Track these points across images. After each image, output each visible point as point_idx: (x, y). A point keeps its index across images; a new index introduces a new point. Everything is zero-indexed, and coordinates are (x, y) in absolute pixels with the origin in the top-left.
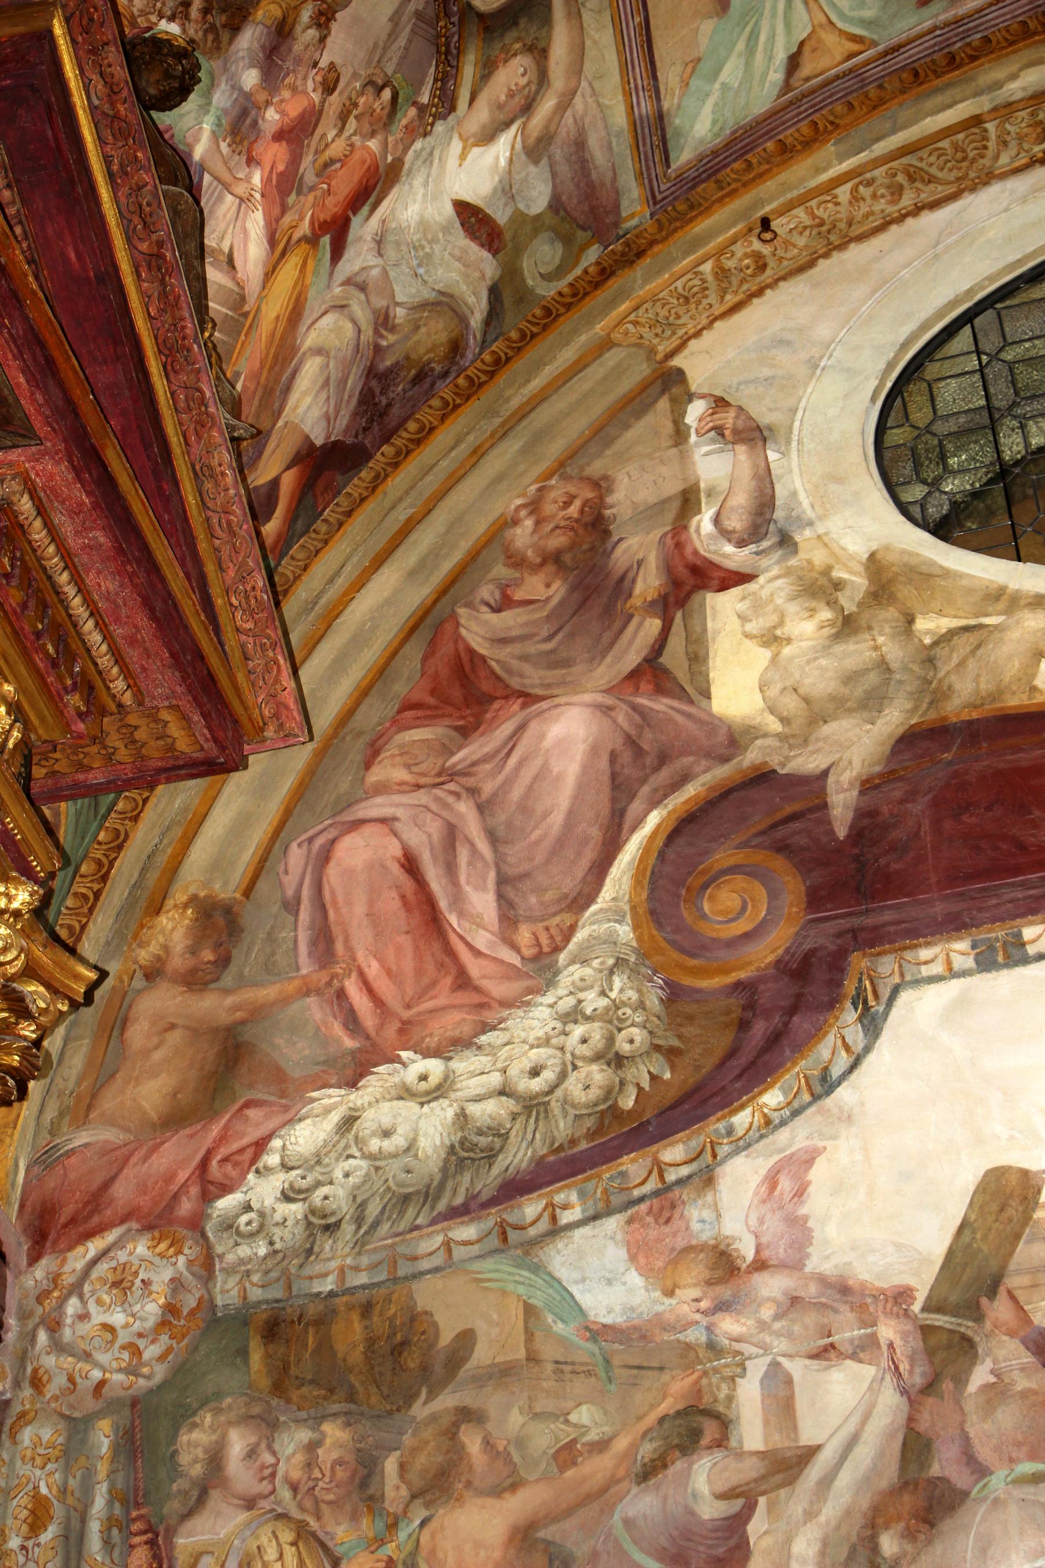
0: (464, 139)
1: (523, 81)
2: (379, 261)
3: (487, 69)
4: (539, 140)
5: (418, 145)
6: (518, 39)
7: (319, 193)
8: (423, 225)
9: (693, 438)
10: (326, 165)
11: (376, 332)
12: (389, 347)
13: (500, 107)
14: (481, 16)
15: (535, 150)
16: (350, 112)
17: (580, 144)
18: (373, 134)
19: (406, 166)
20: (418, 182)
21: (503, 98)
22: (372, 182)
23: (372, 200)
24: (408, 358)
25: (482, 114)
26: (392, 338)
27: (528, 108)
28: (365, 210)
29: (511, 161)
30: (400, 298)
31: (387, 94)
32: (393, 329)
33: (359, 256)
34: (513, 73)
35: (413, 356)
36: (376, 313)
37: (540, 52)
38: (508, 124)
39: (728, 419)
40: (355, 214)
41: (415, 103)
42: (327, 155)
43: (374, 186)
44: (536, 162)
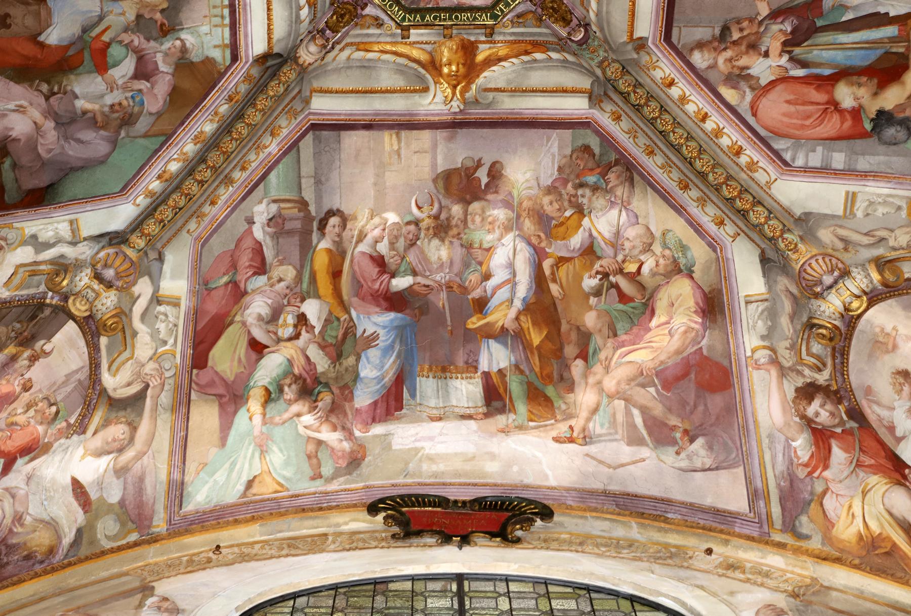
0: (86, 450)
1: (122, 437)
2: (26, 487)
3: (106, 423)
4: (122, 468)
5: (62, 441)
6: (125, 417)
7: (5, 435)
8: (53, 481)
9: (146, 608)
10: (12, 424)
11: (13, 522)
12: (17, 533)
13: (107, 443)
14: (110, 398)
15: (120, 472)
16: (32, 406)
17: (141, 479)
18: (41, 423)
19: (54, 448)
20: (57, 458)
21: (110, 440)
22: (34, 446)
23: (32, 455)
24: (25, 544)
25: (97, 442)
26: (20, 530)
27: (121, 450)
28: (27, 458)
29: (106, 471)
30: (30, 511)
31: (54, 409)
32: (22, 525)
33: (15, 479)
34: (118, 431)
35: (29, 544)
36: (16, 512)
37: (134, 428)
38: (109, 453)
39: (166, 605)
40: (21, 457)
41: (66, 421)
42: (15, 419)
43: (33, 449)
44: (118, 478)
